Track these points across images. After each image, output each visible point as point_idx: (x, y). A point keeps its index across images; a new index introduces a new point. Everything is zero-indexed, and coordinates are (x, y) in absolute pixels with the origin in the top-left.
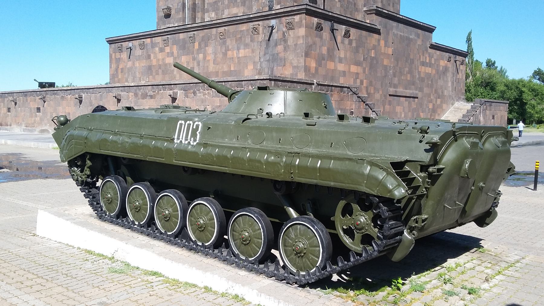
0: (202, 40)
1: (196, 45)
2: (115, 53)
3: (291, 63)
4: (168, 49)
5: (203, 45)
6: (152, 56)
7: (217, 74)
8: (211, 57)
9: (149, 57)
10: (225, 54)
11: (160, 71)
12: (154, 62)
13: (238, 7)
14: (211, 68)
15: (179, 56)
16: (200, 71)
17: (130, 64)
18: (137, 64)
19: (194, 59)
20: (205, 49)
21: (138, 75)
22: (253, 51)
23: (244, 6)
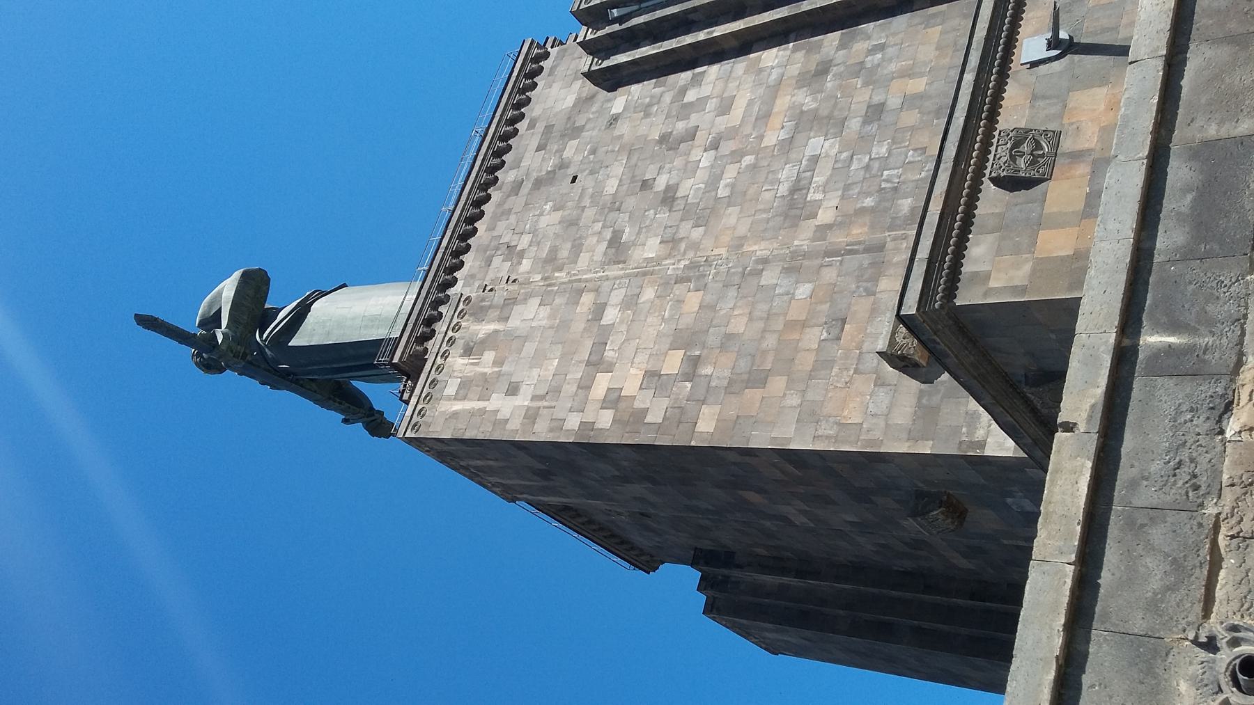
2: (1039, 224)
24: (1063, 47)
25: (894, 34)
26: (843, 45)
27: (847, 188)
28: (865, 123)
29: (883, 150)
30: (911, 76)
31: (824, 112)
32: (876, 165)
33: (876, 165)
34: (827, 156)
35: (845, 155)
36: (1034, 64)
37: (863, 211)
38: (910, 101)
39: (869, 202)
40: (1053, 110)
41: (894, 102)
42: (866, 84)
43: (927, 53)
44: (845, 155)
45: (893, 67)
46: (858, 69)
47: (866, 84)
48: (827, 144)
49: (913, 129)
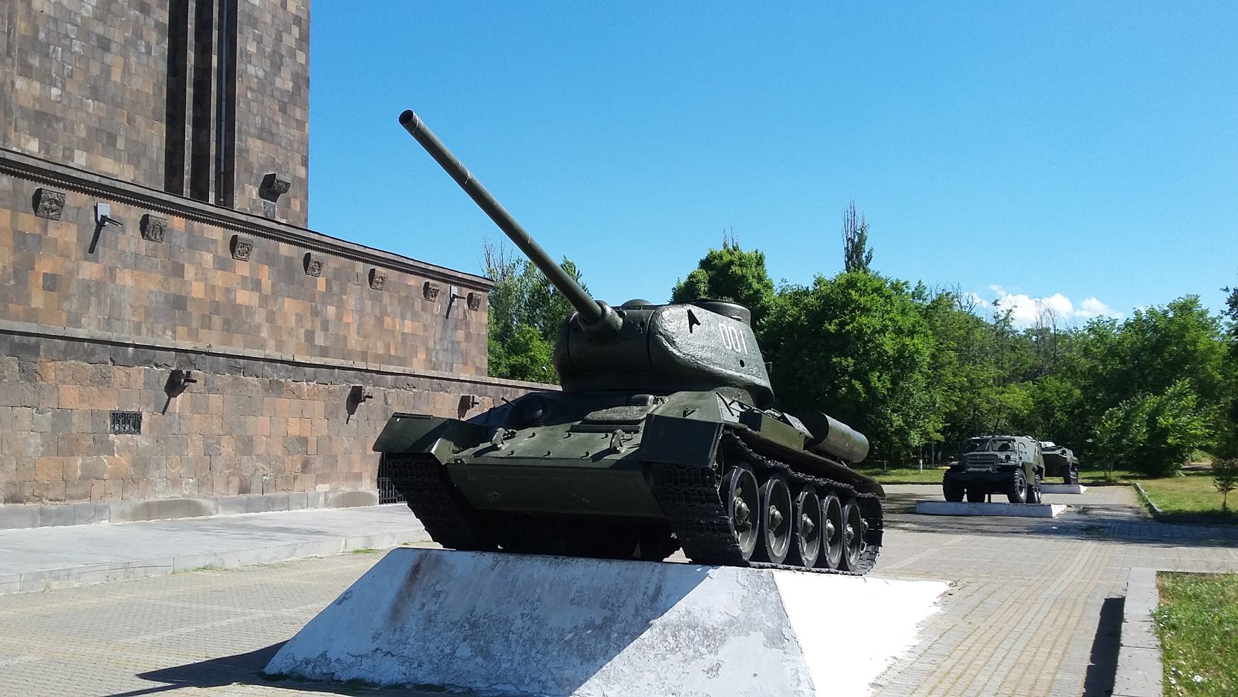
0: (335, 278)
1: (321, 283)
3: (474, 362)
4: (243, 268)
5: (336, 288)
6: (190, 272)
7: (364, 356)
8: (349, 318)
9: (178, 271)
10: (380, 321)
11: (217, 321)
12: (197, 291)
13: (118, 159)
15: (275, 293)
16: (327, 344)
17: (90, 271)
18: (126, 278)
19: (315, 313)
20: (341, 299)
21: (128, 314)
22: (426, 329)
23: (137, 165)
24: (101, 223)
25: (155, 62)
26: (158, 25)
27: (55, 20)
28: (99, 36)
29: (77, 49)
30: (124, 72)
31: (113, 8)
32: (67, 43)
33: (67, 43)
34: (81, 7)
35: (79, 20)
36: (96, 208)
37: (36, 31)
38: (106, 71)
39: (42, 35)
40: (70, 218)
41: (109, 58)
42: (126, 40)
43: (137, 83)
44: (79, 20)
45: (133, 59)
46: (138, 35)
47: (126, 40)
48: (90, 7)
49: (87, 69)
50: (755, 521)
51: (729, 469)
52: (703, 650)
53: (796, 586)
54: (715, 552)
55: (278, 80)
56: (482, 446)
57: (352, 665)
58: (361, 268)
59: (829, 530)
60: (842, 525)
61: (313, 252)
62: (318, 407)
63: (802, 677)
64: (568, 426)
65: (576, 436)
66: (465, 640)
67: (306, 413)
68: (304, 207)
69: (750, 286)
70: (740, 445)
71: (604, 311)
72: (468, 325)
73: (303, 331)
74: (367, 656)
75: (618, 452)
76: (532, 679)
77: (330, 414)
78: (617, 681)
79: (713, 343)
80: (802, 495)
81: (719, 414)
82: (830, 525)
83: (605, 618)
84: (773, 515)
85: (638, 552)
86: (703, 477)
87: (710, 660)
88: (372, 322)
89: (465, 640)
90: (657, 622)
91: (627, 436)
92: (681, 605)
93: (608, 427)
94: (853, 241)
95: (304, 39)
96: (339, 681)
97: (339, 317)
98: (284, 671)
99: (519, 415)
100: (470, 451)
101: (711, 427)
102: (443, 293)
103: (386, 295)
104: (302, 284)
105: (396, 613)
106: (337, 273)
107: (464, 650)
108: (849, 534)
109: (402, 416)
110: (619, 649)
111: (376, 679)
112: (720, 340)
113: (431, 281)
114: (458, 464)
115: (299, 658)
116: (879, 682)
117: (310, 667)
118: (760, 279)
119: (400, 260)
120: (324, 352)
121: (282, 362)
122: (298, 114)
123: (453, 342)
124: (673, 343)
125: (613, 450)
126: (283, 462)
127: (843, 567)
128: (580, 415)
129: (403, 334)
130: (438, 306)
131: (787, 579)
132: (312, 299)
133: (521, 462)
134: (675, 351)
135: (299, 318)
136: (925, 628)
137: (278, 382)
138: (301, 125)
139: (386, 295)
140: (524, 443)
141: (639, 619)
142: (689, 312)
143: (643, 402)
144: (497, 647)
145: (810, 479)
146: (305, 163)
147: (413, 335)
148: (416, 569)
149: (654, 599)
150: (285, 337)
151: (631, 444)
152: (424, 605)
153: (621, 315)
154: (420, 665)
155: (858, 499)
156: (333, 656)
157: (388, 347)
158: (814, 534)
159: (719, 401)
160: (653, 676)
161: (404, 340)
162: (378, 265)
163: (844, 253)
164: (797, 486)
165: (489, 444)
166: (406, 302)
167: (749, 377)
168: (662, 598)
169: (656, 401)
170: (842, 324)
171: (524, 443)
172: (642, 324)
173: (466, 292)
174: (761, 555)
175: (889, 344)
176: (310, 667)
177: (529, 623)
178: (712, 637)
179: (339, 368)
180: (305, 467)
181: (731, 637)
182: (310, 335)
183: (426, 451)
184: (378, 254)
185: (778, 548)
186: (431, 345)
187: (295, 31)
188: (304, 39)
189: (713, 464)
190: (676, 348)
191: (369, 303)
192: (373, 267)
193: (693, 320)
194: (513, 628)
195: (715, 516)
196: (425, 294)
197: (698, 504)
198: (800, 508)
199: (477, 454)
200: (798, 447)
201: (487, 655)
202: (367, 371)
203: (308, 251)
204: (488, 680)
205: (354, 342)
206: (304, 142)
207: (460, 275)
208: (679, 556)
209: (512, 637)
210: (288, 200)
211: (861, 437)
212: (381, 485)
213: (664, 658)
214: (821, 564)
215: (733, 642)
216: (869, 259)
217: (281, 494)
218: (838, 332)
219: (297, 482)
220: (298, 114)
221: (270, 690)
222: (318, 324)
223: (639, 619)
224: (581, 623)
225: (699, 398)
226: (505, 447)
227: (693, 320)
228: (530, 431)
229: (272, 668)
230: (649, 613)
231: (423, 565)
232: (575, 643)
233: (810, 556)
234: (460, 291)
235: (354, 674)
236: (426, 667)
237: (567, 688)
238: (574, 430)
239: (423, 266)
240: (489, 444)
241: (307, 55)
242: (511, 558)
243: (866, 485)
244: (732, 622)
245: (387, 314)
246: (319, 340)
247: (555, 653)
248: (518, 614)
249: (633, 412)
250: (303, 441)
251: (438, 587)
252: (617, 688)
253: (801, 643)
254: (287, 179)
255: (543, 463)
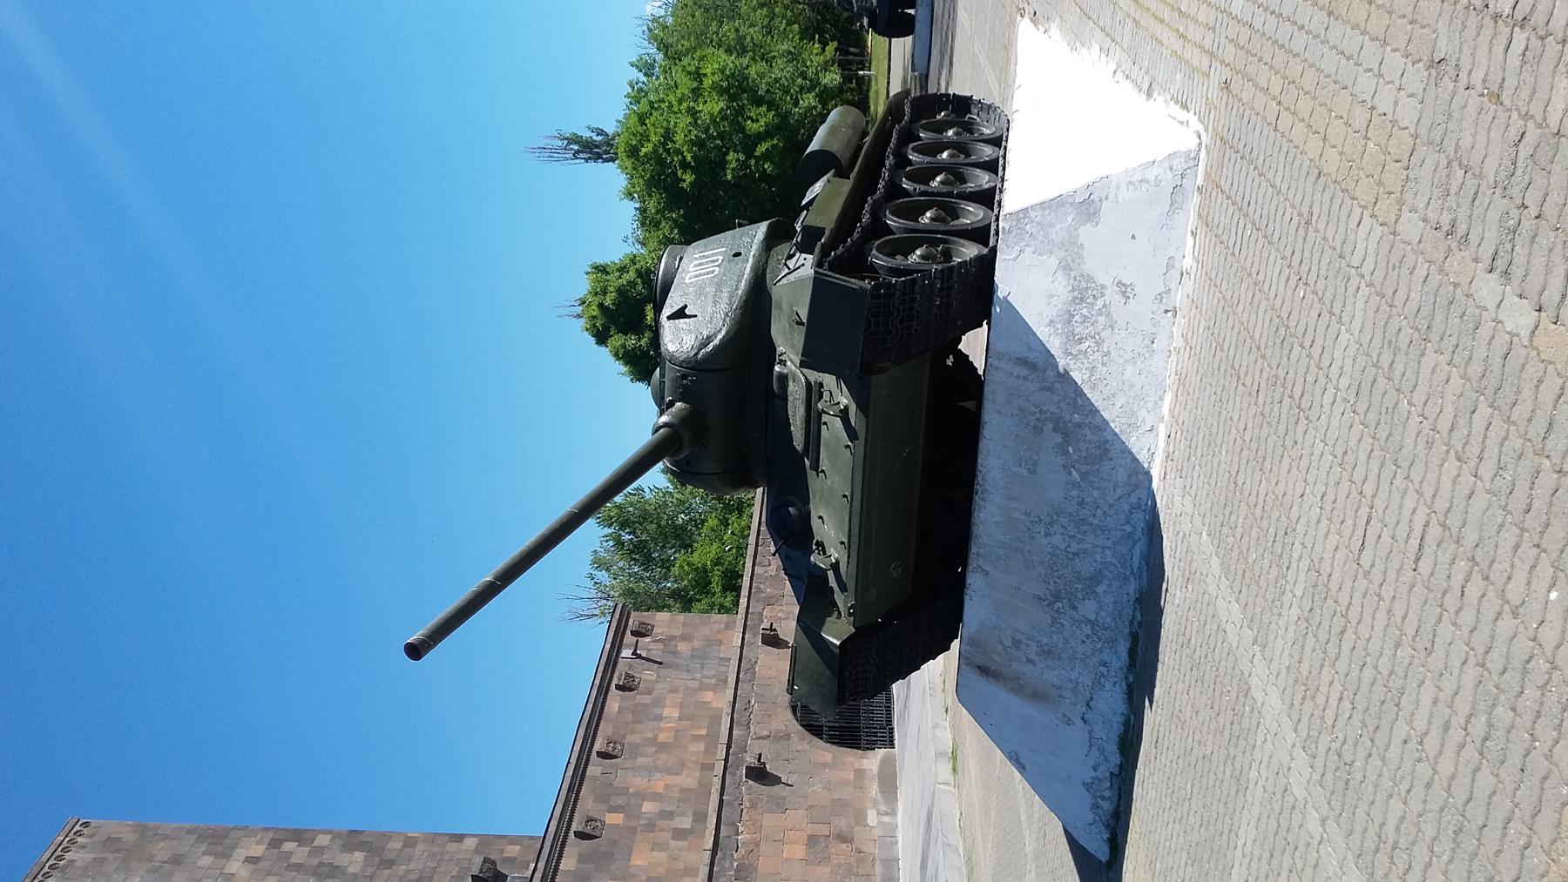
1: (613, 819)
5: (621, 801)
7: (707, 768)
8: (659, 786)
10: (663, 747)
14: (689, 780)
16: (690, 812)
19: (650, 827)
20: (634, 794)
22: (674, 690)
50: (938, 240)
51: (873, 269)
52: (1099, 303)
53: (1020, 188)
54: (975, 294)
55: (351, 870)
56: (833, 583)
57: (1102, 751)
58: (594, 770)
59: (951, 156)
60: (946, 144)
61: (574, 827)
62: (770, 821)
63: (1138, 177)
64: (811, 474)
65: (824, 464)
66: (1075, 608)
67: (778, 836)
68: (515, 840)
69: (632, 284)
70: (843, 251)
71: (665, 425)
72: (672, 638)
73: (673, 843)
74: (1090, 732)
75: (846, 408)
76: (1128, 522)
77: (781, 806)
78: (1134, 414)
79: (710, 290)
80: (906, 185)
81: (801, 281)
82: (945, 155)
83: (1054, 430)
84: (932, 219)
85: (970, 405)
86: (882, 298)
87: (1112, 295)
88: (663, 756)
89: (1075, 608)
90: (1062, 363)
91: (826, 396)
92: (1042, 332)
93: (813, 421)
94: (578, 152)
95: (299, 836)
96: (1121, 766)
97: (656, 797)
98: (1106, 836)
99: (793, 535)
100: (839, 597)
101: (818, 282)
102: (630, 667)
103: (630, 739)
104: (614, 843)
105: (1037, 696)
106: (601, 798)
107: (1088, 608)
108: (956, 134)
109: (791, 682)
110: (1094, 411)
111: (1121, 719)
112: (704, 286)
113: (615, 681)
114: (855, 612)
115: (1090, 817)
116: (1145, 87)
117: (1103, 803)
118: (623, 269)
119: (586, 719)
120: (700, 817)
121: (712, 864)
122: (396, 845)
123: (693, 657)
124: (709, 339)
125: (844, 415)
126: (839, 865)
127: (997, 141)
128: (795, 460)
129: (680, 718)
130: (647, 674)
131: (1012, 200)
132: (633, 830)
133: (855, 531)
134: (720, 336)
135: (657, 846)
136: (1077, 39)
137: (738, 870)
138: (409, 842)
139: (630, 739)
140: (831, 530)
141: (1057, 385)
142: (669, 318)
143: (784, 379)
144: (1086, 567)
145: (886, 174)
146: (459, 838)
147: (682, 706)
148: (984, 671)
149: (1033, 367)
150: (681, 865)
151: (836, 392)
152: (1030, 661)
153: (671, 404)
154: (1105, 664)
155: (912, 121)
156: (1088, 775)
157: (696, 738)
158: (956, 174)
159: (784, 281)
160: (1130, 368)
161: (688, 719)
162: (592, 747)
163: (592, 164)
164: (895, 191)
165: (830, 574)
166: (640, 714)
167: (755, 247)
168: (1032, 356)
169: (783, 363)
170: (685, 165)
171: (831, 530)
172: (684, 377)
173: (629, 639)
174: (981, 234)
175: (713, 106)
176: (1103, 803)
177: (1057, 528)
178: (1084, 292)
179: (722, 794)
180: (844, 838)
181: (1085, 268)
182: (679, 834)
183: (837, 651)
184: (578, 747)
185: (973, 214)
186: (695, 684)
187: (288, 846)
188: (299, 836)
189: (867, 284)
190: (715, 335)
191: (640, 760)
192: (594, 753)
193: (680, 314)
194: (1063, 546)
195: (932, 285)
196: (631, 689)
197: (916, 306)
198: (923, 188)
199: (843, 588)
200: (846, 186)
201: (1096, 579)
202: (726, 760)
203: (571, 834)
204: (1126, 579)
205: (689, 780)
206: (433, 838)
207: (608, 646)
208: (974, 344)
209: (1074, 547)
210: (506, 860)
211: (834, 115)
212: (871, 747)
213: (1108, 353)
214: (993, 166)
215: (1091, 265)
216: (600, 132)
217: (878, 869)
218: (694, 170)
219: (865, 848)
220: (396, 845)
221: (1129, 851)
222: (664, 823)
223: (1057, 385)
224: (1060, 460)
225: (780, 308)
226: (835, 553)
227: (680, 314)
228: (815, 523)
229: (1101, 852)
230: (1051, 373)
231: (979, 662)
232: (1084, 468)
233: (984, 179)
234: (628, 647)
235: (1112, 748)
236: (1106, 656)
237: (1141, 477)
238: (816, 466)
239: (594, 692)
240: (830, 574)
241: (319, 832)
242: (974, 549)
243: (895, 109)
244: (1066, 268)
245: (655, 737)
246: (685, 822)
247: (1096, 493)
248: (1045, 541)
249: (796, 392)
250: (812, 840)
251: (1008, 642)
252: (1142, 414)
253: (1089, 180)
254: (479, 860)
255: (857, 504)
